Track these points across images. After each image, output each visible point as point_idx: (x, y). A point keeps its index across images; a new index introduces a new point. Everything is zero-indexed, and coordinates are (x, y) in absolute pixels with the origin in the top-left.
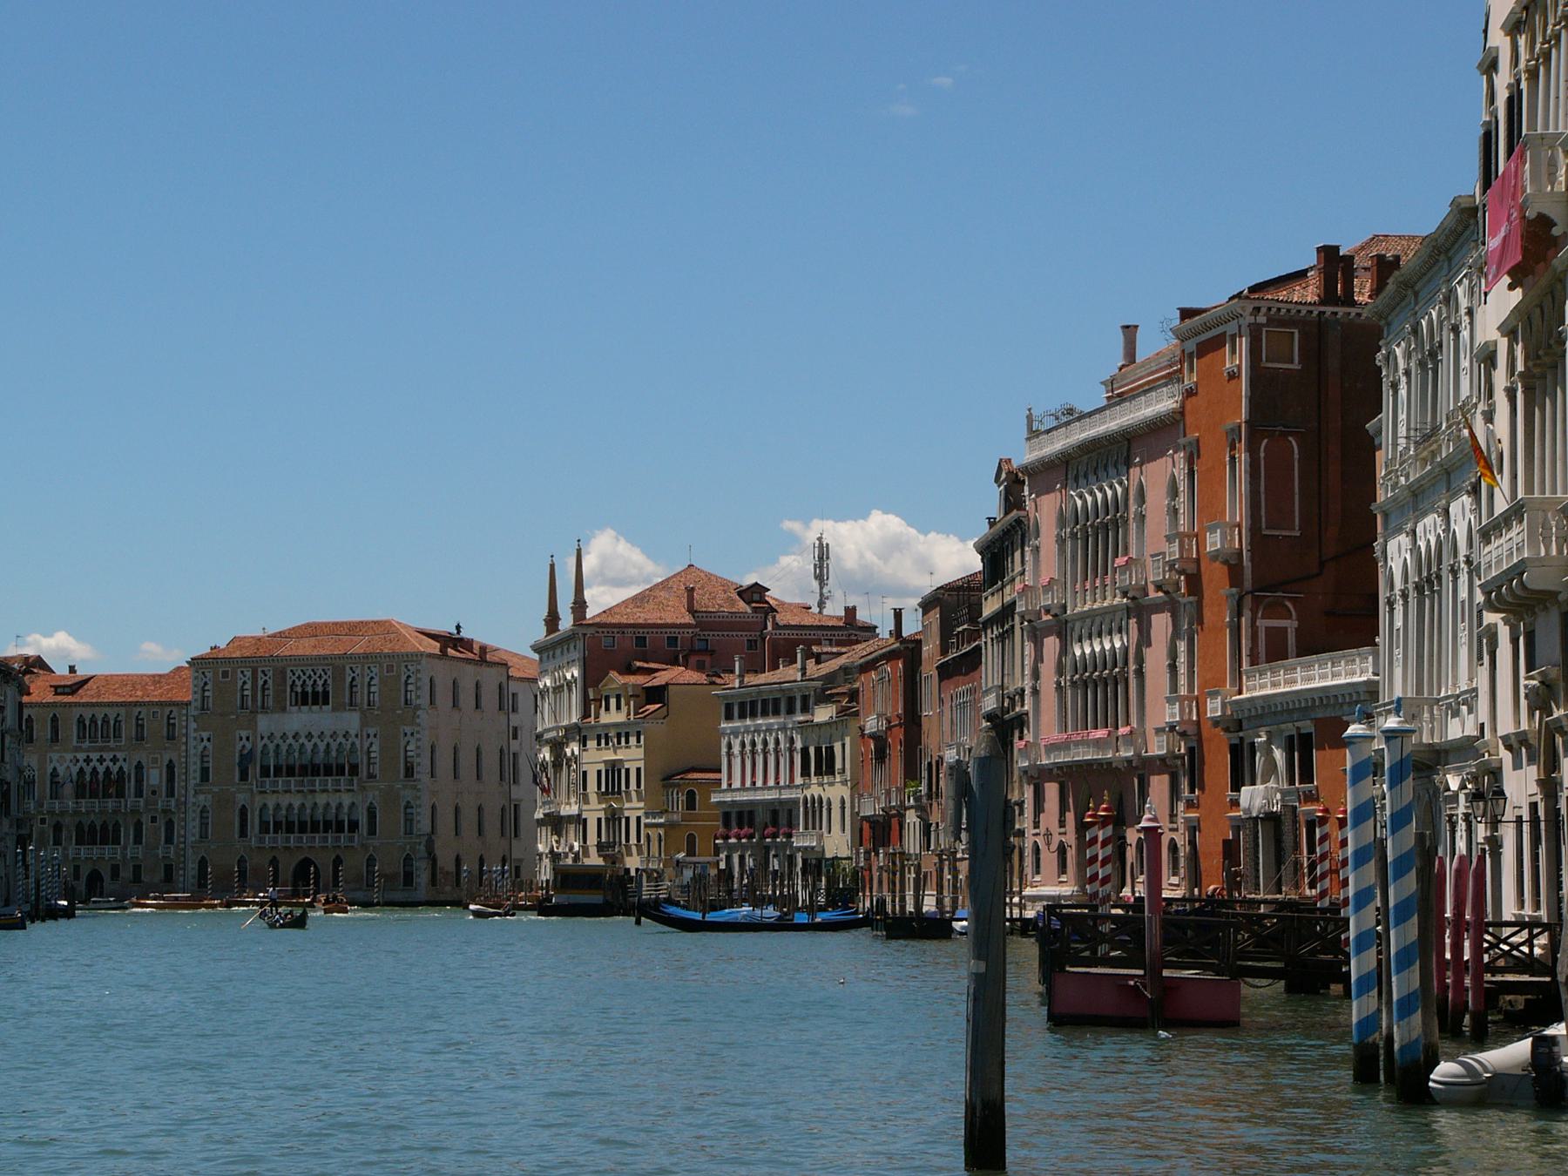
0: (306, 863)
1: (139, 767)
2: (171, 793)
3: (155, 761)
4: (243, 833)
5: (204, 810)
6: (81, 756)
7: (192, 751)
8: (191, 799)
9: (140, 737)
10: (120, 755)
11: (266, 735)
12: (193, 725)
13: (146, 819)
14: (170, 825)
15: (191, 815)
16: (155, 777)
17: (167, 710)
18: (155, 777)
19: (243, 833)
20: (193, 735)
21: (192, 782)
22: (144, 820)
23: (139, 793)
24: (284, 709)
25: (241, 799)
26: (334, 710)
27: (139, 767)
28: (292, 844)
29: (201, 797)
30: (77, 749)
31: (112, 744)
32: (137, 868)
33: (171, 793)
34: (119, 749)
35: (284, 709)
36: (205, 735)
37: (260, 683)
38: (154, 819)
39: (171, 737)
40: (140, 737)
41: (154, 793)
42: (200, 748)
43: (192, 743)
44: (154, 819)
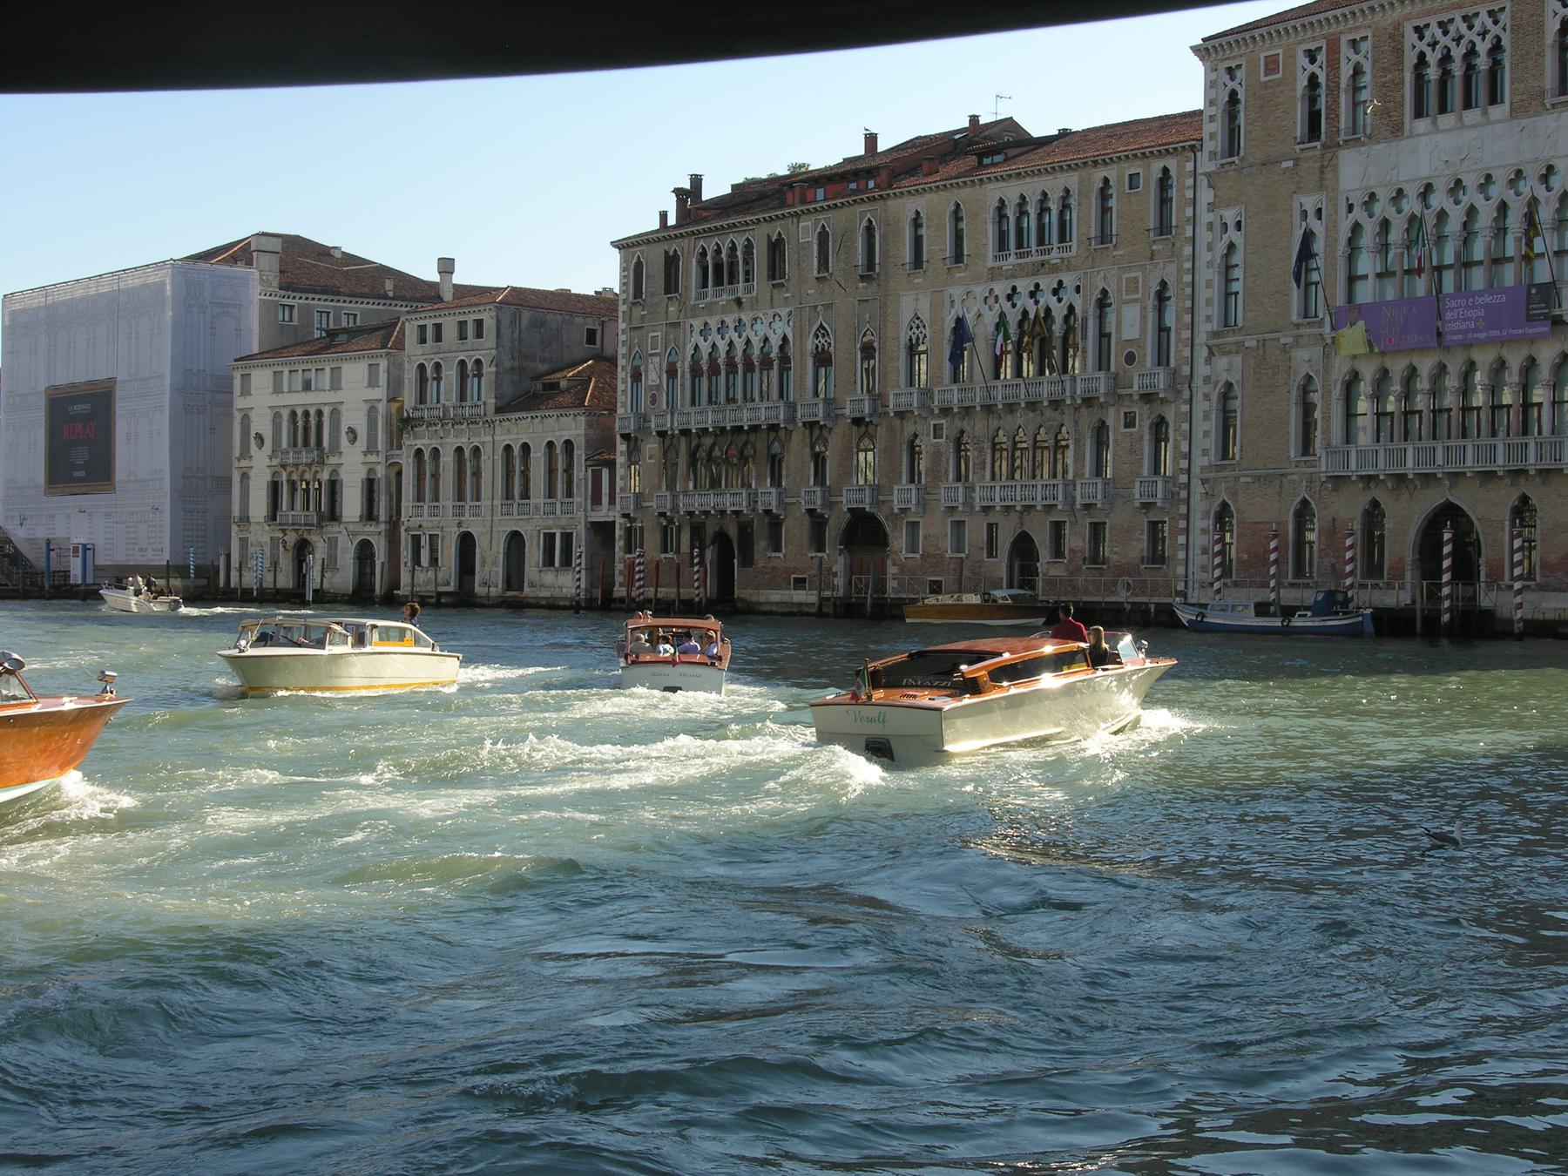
0: (1449, 513)
1: (1102, 303)
2: (1162, 357)
3: (1133, 285)
4: (1306, 446)
5: (1227, 394)
6: (1001, 288)
7: (1204, 257)
8: (1202, 370)
9: (1104, 237)
10: (1069, 280)
11: (1357, 199)
12: (1206, 196)
13: (1113, 418)
14: (1159, 429)
15: (1200, 406)
16: (1130, 323)
17: (1157, 166)
18: (1130, 323)
19: (1306, 446)
20: (1205, 217)
21: (1203, 329)
22: (1110, 422)
23: (1103, 363)
24: (1397, 130)
25: (1304, 359)
26: (1514, 113)
27: (1102, 303)
28: (1410, 467)
29: (1222, 362)
30: (994, 274)
31: (1054, 257)
32: (1097, 529)
33: (1162, 357)
34: (1067, 265)
35: (1397, 130)
36: (1230, 215)
37: (1346, 72)
38: (1130, 422)
39: (1164, 227)
40: (1104, 237)
41: (1130, 358)
42: (1221, 248)
43: (1204, 237)
44: (1130, 422)
